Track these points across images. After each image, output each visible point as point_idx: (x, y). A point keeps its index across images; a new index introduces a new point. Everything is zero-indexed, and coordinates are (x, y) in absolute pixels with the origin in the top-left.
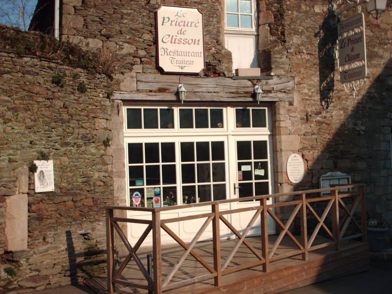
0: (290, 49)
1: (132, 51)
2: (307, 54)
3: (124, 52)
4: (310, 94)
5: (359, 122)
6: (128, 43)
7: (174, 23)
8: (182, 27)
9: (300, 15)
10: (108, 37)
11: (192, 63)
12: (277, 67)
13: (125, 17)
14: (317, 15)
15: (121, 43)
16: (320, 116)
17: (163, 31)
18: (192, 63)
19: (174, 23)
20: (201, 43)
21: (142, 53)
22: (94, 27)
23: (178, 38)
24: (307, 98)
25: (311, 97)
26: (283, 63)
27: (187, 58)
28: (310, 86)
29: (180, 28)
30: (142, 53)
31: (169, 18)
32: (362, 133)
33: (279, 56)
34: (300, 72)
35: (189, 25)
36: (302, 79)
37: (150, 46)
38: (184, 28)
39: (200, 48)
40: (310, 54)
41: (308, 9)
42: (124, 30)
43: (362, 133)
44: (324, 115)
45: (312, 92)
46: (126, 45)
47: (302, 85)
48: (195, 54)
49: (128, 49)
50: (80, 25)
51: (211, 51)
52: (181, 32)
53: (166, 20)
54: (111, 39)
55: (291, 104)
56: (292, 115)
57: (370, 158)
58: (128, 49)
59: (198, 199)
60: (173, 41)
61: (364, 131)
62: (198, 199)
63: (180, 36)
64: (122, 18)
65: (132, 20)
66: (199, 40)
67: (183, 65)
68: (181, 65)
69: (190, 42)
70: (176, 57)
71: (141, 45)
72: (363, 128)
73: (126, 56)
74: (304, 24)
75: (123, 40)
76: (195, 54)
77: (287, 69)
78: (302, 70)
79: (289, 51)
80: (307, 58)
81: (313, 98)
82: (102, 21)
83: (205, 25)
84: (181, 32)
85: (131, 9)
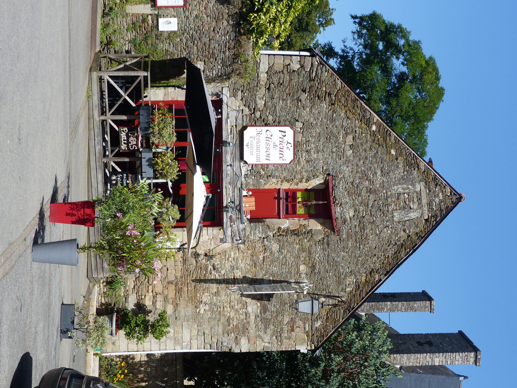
0: (267, 241)
1: (259, 106)
2: (264, 257)
3: (259, 101)
4: (230, 259)
5: (207, 307)
6: (265, 104)
7: (281, 140)
8: (279, 147)
9: (296, 251)
10: (269, 89)
11: (252, 154)
12: (251, 228)
13: (284, 102)
14: (297, 267)
15: (264, 99)
16: (212, 269)
17: (275, 130)
18: (252, 154)
19: (281, 140)
20: (267, 162)
21: (258, 114)
22: (275, 79)
23: (270, 143)
24: (227, 256)
25: (228, 260)
26: (255, 234)
27: (255, 149)
28: (237, 259)
29: (278, 145)
30: (258, 114)
31: (285, 136)
32: (198, 310)
33: (261, 230)
34: (248, 250)
35: (281, 153)
36: (242, 252)
37: (264, 121)
38: (278, 148)
39: (263, 161)
40: (264, 260)
41: (302, 259)
42: (275, 101)
43: (198, 310)
44: (213, 272)
45: (231, 262)
46: (263, 102)
47: (237, 251)
48: (258, 158)
49: (261, 103)
50: (277, 68)
51: (262, 170)
52: (275, 146)
53: (284, 134)
54: (267, 91)
55: (222, 241)
56: (212, 242)
57: (176, 318)
58: (261, 103)
59: (150, 63)
60: (267, 139)
61: (199, 312)
62: (150, 63)
63: (272, 144)
64: (283, 100)
65: (282, 107)
66: (269, 160)
67: (249, 146)
68: (249, 144)
69: (267, 153)
70: (256, 141)
71: (264, 114)
72: (202, 312)
73: (255, 103)
74: (289, 255)
75: (267, 100)
76: (258, 158)
77: (251, 237)
78: (250, 252)
79: (265, 239)
80: (260, 257)
81: (227, 261)
82: (280, 84)
83: (281, 165)
84: (275, 146)
85: (290, 107)
